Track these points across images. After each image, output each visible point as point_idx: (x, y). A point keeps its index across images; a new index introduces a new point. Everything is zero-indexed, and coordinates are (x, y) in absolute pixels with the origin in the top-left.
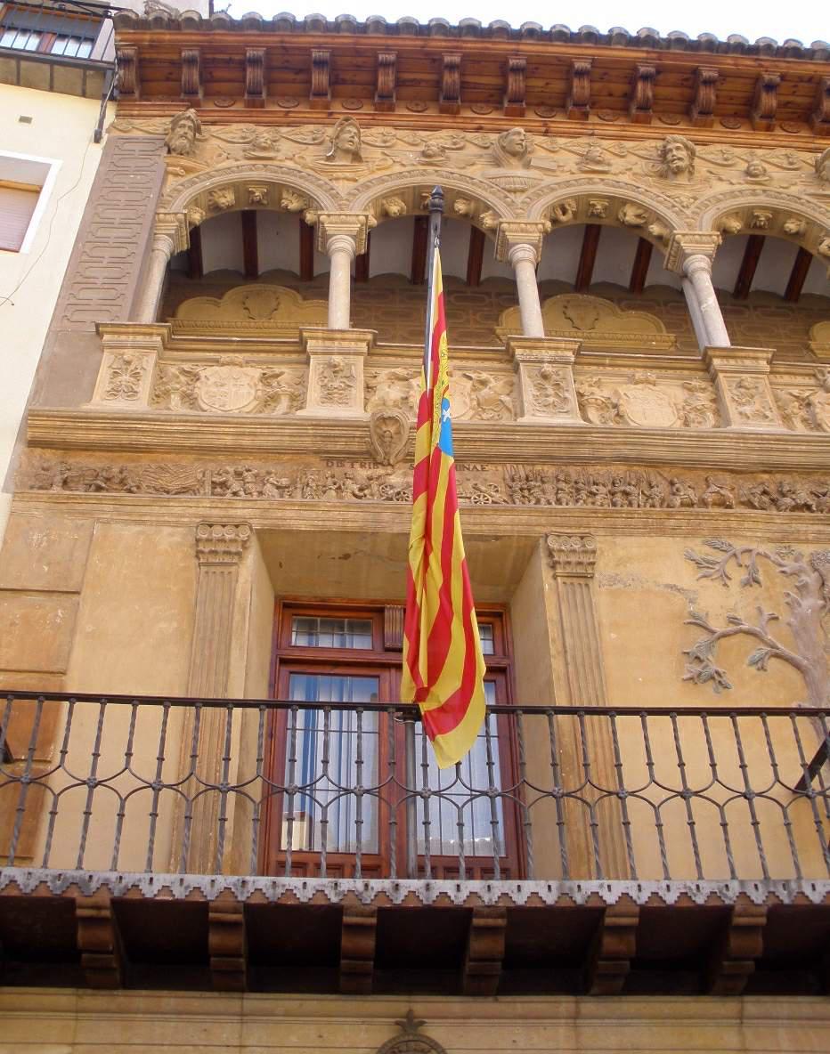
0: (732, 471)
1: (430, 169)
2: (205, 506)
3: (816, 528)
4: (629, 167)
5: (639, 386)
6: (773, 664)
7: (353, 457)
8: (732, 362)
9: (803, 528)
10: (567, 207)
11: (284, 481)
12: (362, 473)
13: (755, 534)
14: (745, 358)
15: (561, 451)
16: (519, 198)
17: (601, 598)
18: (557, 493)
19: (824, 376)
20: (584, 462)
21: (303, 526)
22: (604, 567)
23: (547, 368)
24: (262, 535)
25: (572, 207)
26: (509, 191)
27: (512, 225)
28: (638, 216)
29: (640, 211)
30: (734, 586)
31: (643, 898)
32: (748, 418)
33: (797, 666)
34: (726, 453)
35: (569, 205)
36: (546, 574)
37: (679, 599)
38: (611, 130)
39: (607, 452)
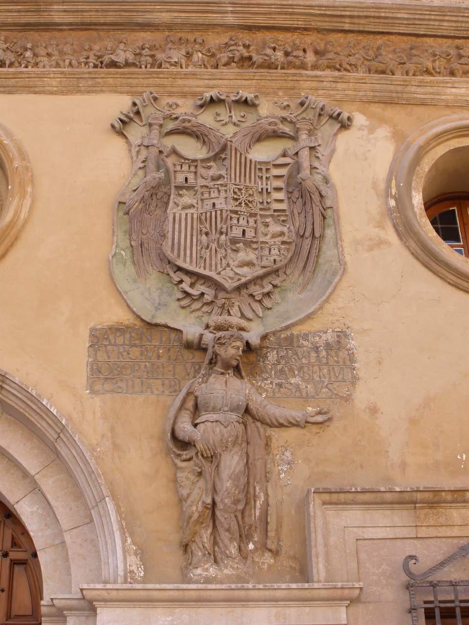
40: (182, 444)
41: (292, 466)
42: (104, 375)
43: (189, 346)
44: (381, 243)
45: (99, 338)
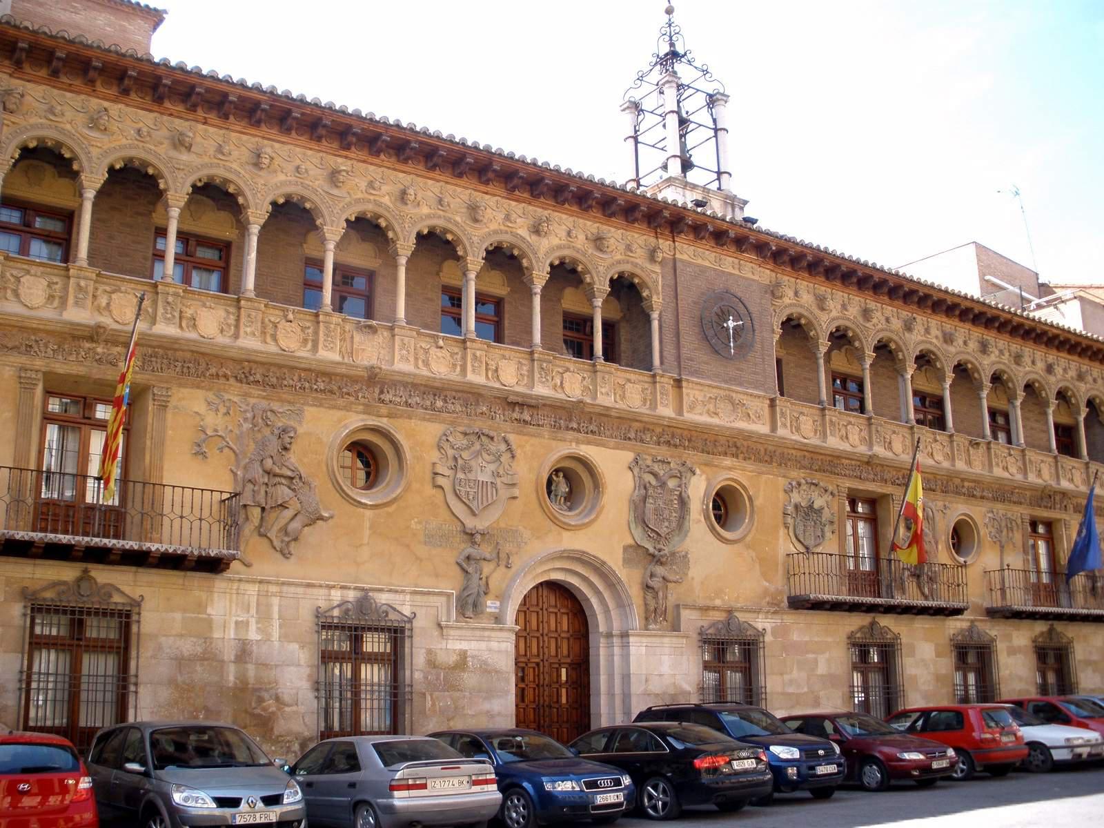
1: (141, 144)
2: (24, 360)
6: (226, 450)
7: (84, 338)
9: (253, 391)
11: (56, 347)
12: (87, 345)
13: (234, 393)
16: (181, 174)
17: (169, 416)
20: (176, 350)
21: (61, 371)
22: (173, 402)
23: (170, 299)
24: (45, 373)
25: (205, 180)
30: (220, 415)
31: (163, 550)
33: (234, 452)
34: (233, 353)
36: (151, 402)
37: (198, 418)
38: (238, 128)
39: (186, 348)
40: (648, 587)
41: (673, 596)
42: (627, 562)
43: (650, 554)
44: (700, 521)
45: (626, 548)
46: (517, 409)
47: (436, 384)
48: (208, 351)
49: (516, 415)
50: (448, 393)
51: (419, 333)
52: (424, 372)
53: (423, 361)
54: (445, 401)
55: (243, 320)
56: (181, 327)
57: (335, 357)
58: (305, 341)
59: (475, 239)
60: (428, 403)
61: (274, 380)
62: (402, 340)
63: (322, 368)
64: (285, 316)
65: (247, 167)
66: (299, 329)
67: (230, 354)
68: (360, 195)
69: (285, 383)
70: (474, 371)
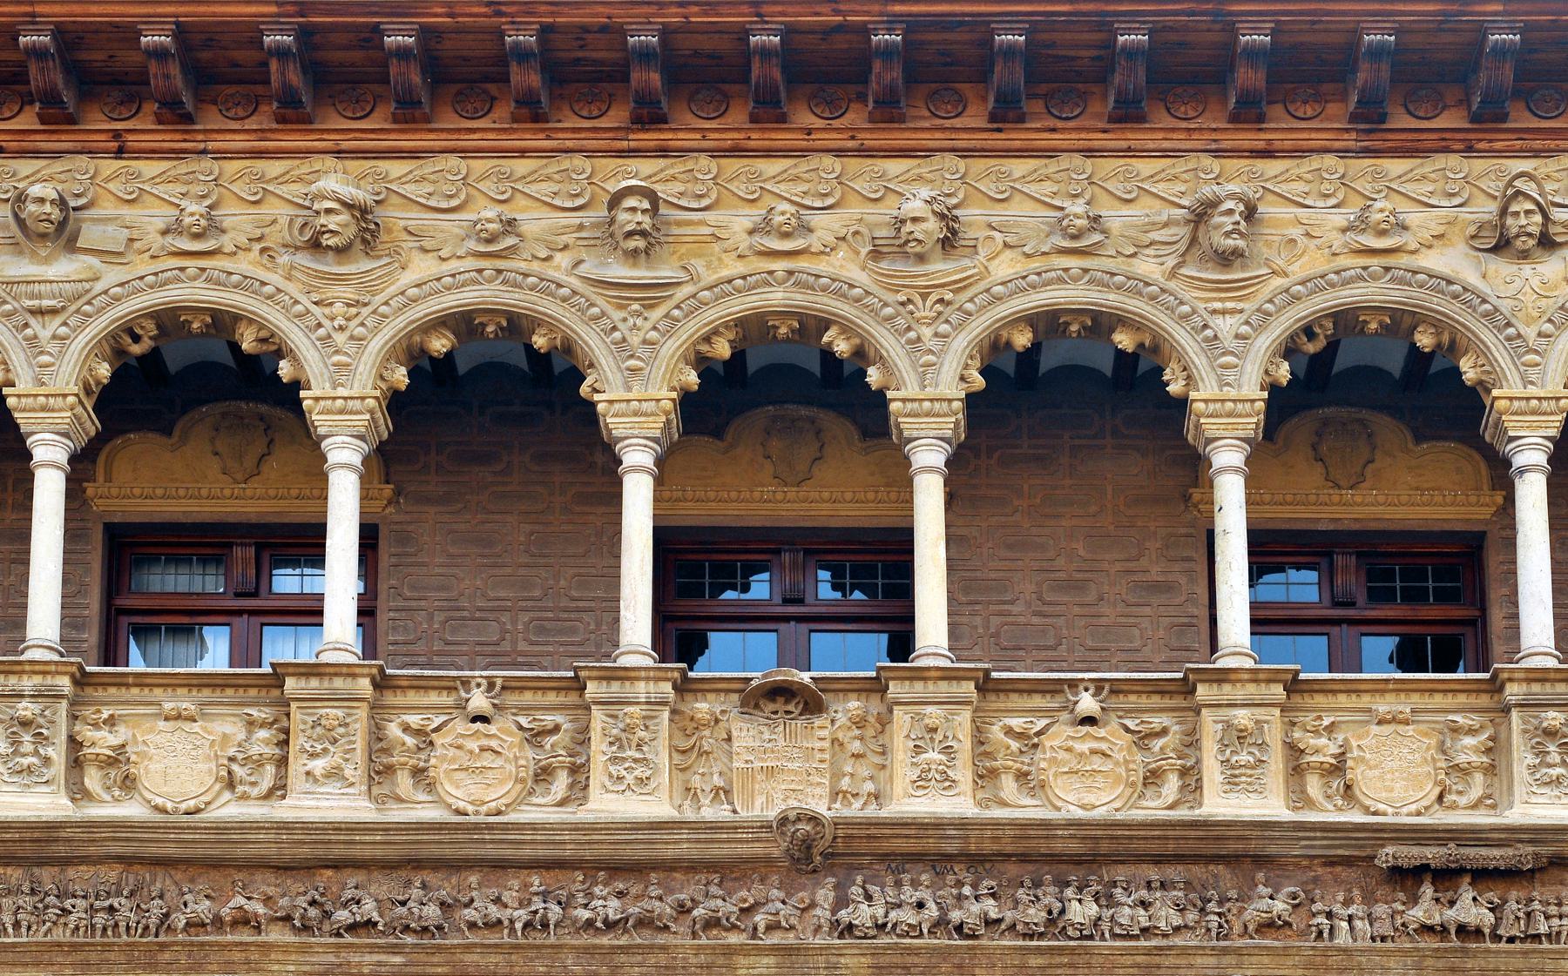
0: (278, 868)
3: (376, 958)
4: (258, 233)
5: (171, 723)
8: (314, 682)
10: (139, 331)
14: (336, 675)
15: (28, 850)
18: (16, 913)
19: (468, 691)
26: (35, 312)
27: (23, 400)
28: (263, 341)
29: (263, 334)
32: (316, 781)
35: (142, 328)
46: (1427, 891)
47: (1059, 847)
48: (171, 850)
49: (1425, 910)
50: (1121, 873)
51: (986, 686)
52: (1028, 809)
53: (1022, 776)
54: (1105, 899)
55: (298, 741)
56: (78, 793)
57: (657, 807)
58: (544, 775)
59: (1226, 326)
60: (1036, 915)
61: (432, 912)
62: (918, 718)
63: (604, 852)
64: (462, 706)
65: (284, 259)
66: (516, 738)
67: (252, 851)
68: (733, 268)
69: (470, 914)
70: (1232, 782)
